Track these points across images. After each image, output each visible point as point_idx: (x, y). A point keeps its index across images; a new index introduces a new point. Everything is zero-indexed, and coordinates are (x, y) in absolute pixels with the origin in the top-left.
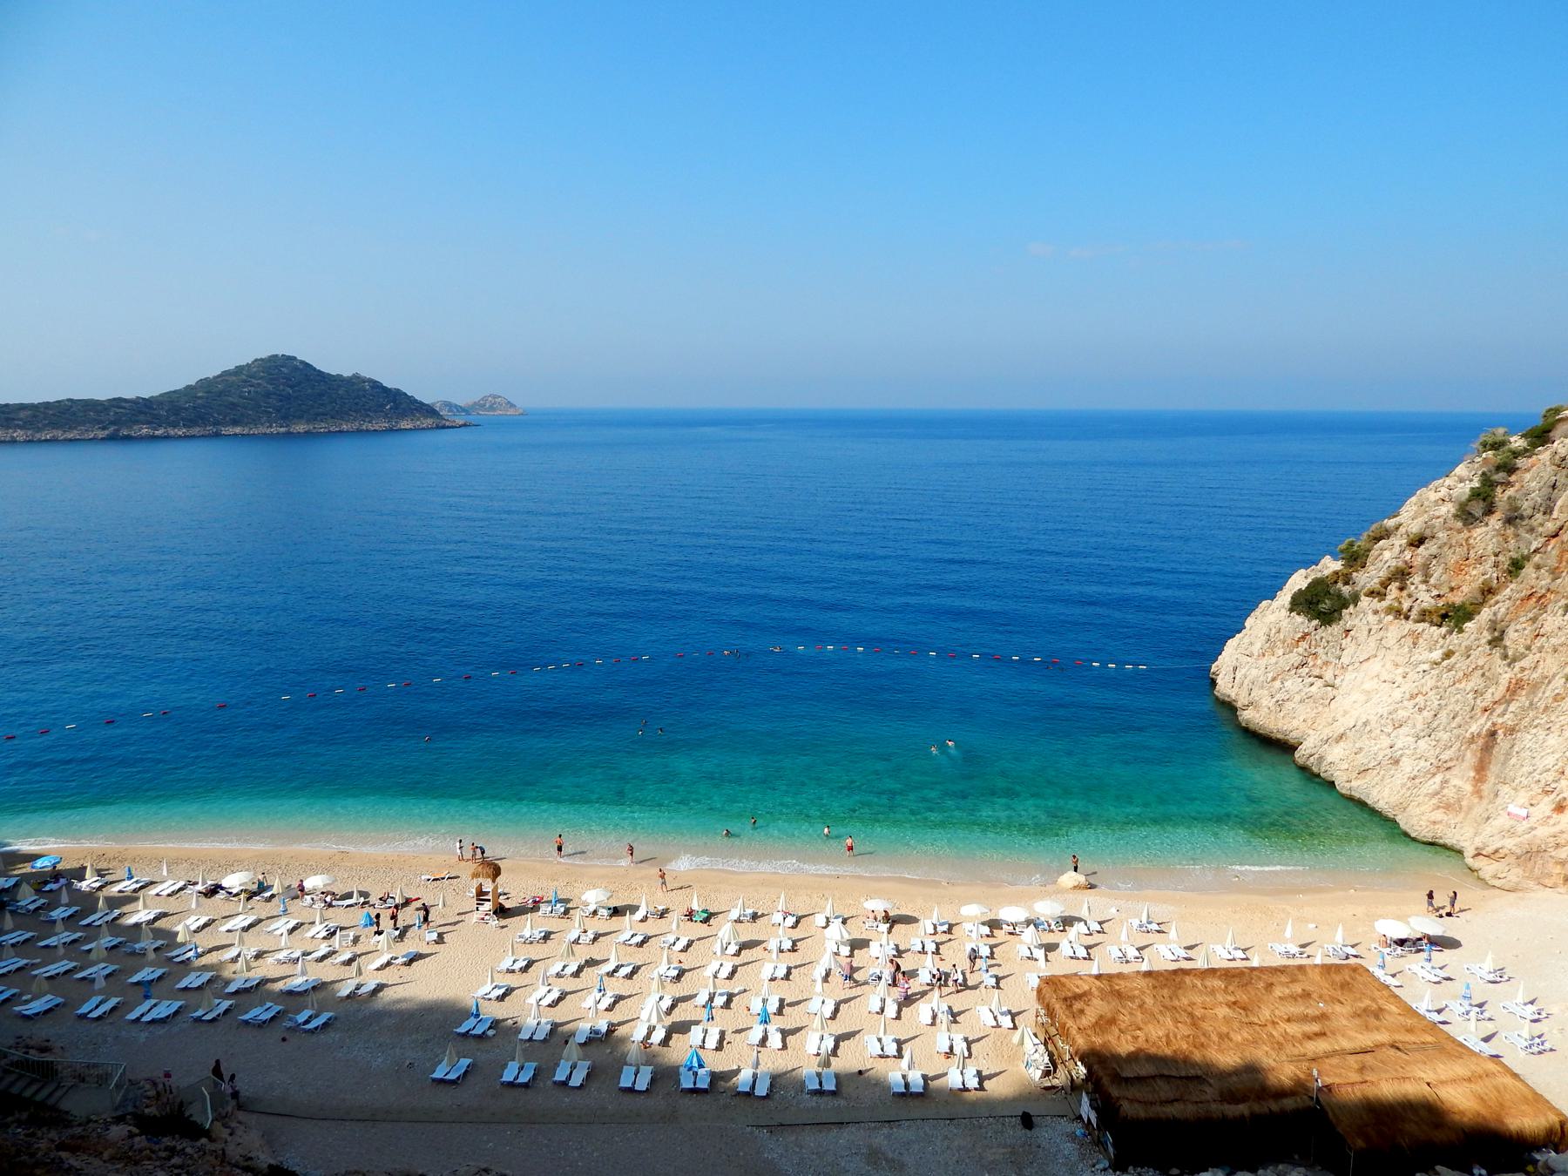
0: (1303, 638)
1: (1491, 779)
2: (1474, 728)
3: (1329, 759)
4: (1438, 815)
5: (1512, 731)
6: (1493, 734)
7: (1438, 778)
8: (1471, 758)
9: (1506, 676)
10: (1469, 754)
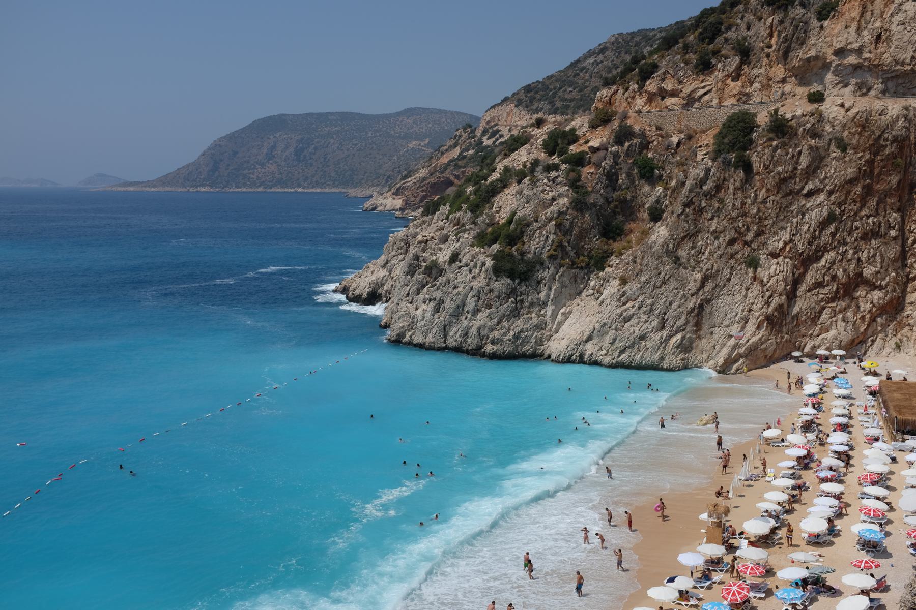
0: (511, 292)
1: (705, 328)
2: (691, 305)
3: (588, 353)
4: (682, 356)
5: (709, 301)
6: (701, 306)
7: (679, 336)
8: (692, 321)
9: (698, 276)
10: (691, 319)
